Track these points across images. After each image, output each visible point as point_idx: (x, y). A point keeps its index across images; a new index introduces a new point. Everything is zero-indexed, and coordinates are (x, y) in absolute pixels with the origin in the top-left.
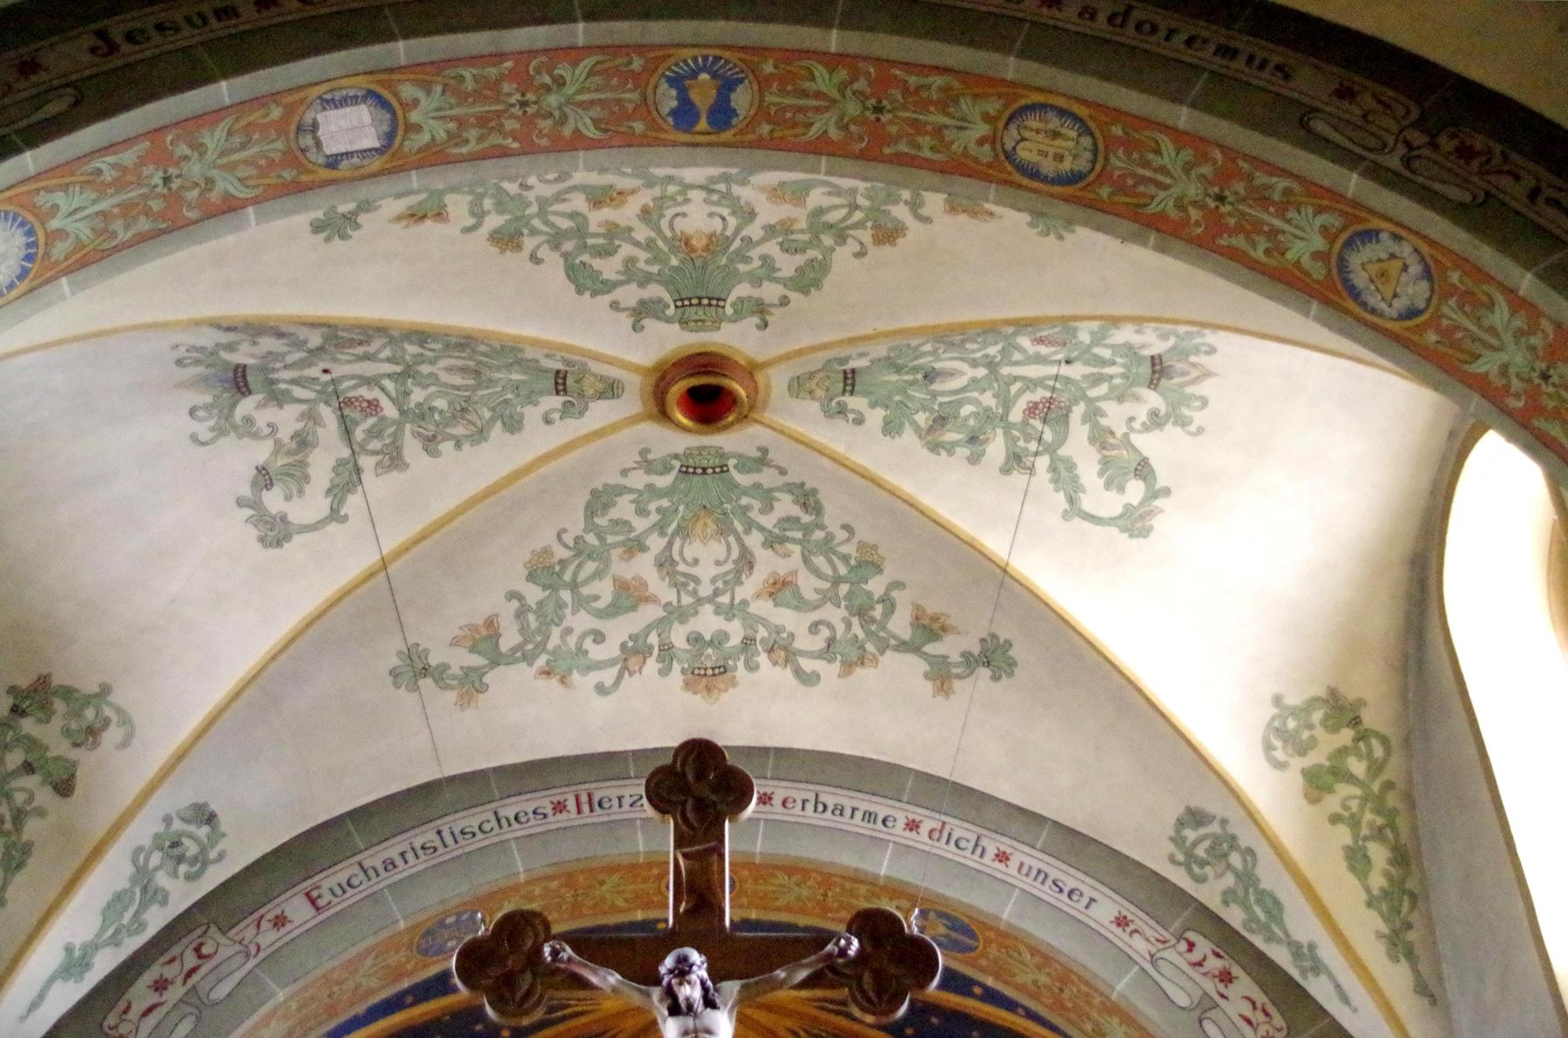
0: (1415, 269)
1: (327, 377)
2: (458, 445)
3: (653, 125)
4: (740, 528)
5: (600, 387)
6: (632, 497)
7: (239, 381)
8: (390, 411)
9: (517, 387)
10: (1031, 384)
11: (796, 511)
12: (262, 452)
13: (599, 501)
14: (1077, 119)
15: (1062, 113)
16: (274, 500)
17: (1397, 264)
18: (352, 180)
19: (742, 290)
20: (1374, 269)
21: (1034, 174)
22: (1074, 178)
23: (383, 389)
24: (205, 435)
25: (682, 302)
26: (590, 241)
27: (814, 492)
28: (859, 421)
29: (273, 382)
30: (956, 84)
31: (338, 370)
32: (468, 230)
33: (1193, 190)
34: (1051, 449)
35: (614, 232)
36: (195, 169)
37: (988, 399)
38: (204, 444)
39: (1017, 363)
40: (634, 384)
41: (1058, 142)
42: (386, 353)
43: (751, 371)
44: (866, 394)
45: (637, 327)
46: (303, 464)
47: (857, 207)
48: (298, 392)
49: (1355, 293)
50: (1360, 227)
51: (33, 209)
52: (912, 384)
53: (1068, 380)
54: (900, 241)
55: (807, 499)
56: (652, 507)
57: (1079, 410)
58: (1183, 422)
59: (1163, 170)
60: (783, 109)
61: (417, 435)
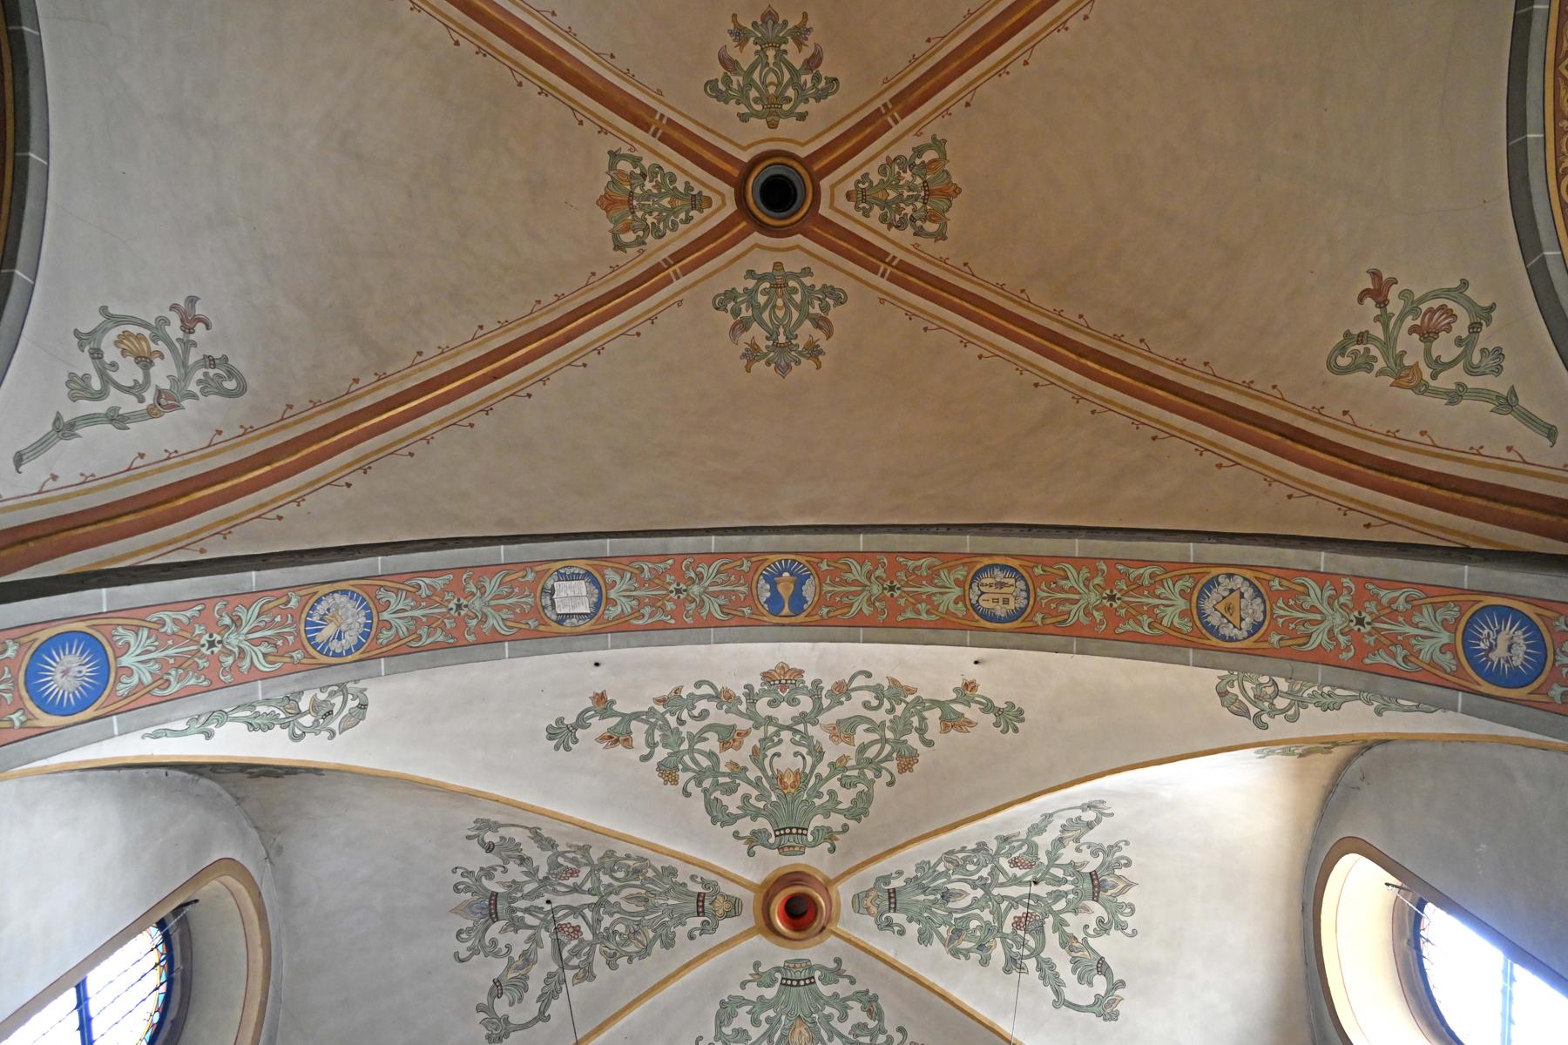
0: (1248, 593)
1: (548, 907)
2: (630, 960)
3: (755, 610)
4: (825, 1037)
5: (726, 905)
6: (748, 1008)
7: (491, 908)
8: (587, 935)
9: (672, 909)
10: (1015, 902)
11: (864, 1018)
12: (498, 967)
13: (726, 1011)
14: (1013, 569)
15: (1003, 568)
16: (502, 1007)
17: (1236, 595)
18: (572, 634)
19: (818, 821)
20: (1221, 607)
21: (990, 617)
22: (1018, 614)
23: (584, 918)
24: (464, 954)
25: (780, 832)
26: (722, 780)
27: (876, 997)
28: (902, 932)
29: (514, 910)
30: (937, 562)
31: (558, 901)
32: (645, 758)
33: (1093, 598)
34: (1035, 953)
35: (737, 771)
36: (477, 604)
37: (987, 915)
38: (462, 961)
39: (1002, 885)
40: (748, 898)
41: (1005, 590)
42: (588, 886)
43: (826, 886)
44: (905, 911)
45: (751, 854)
46: (525, 977)
47: (887, 741)
48: (530, 920)
49: (1213, 630)
50: (1204, 580)
51: (375, 600)
52: (935, 902)
53: (1038, 898)
54: (915, 767)
55: (871, 1005)
56: (763, 1017)
57: (1049, 921)
58: (1122, 927)
59: (1072, 590)
60: (834, 594)
61: (603, 953)
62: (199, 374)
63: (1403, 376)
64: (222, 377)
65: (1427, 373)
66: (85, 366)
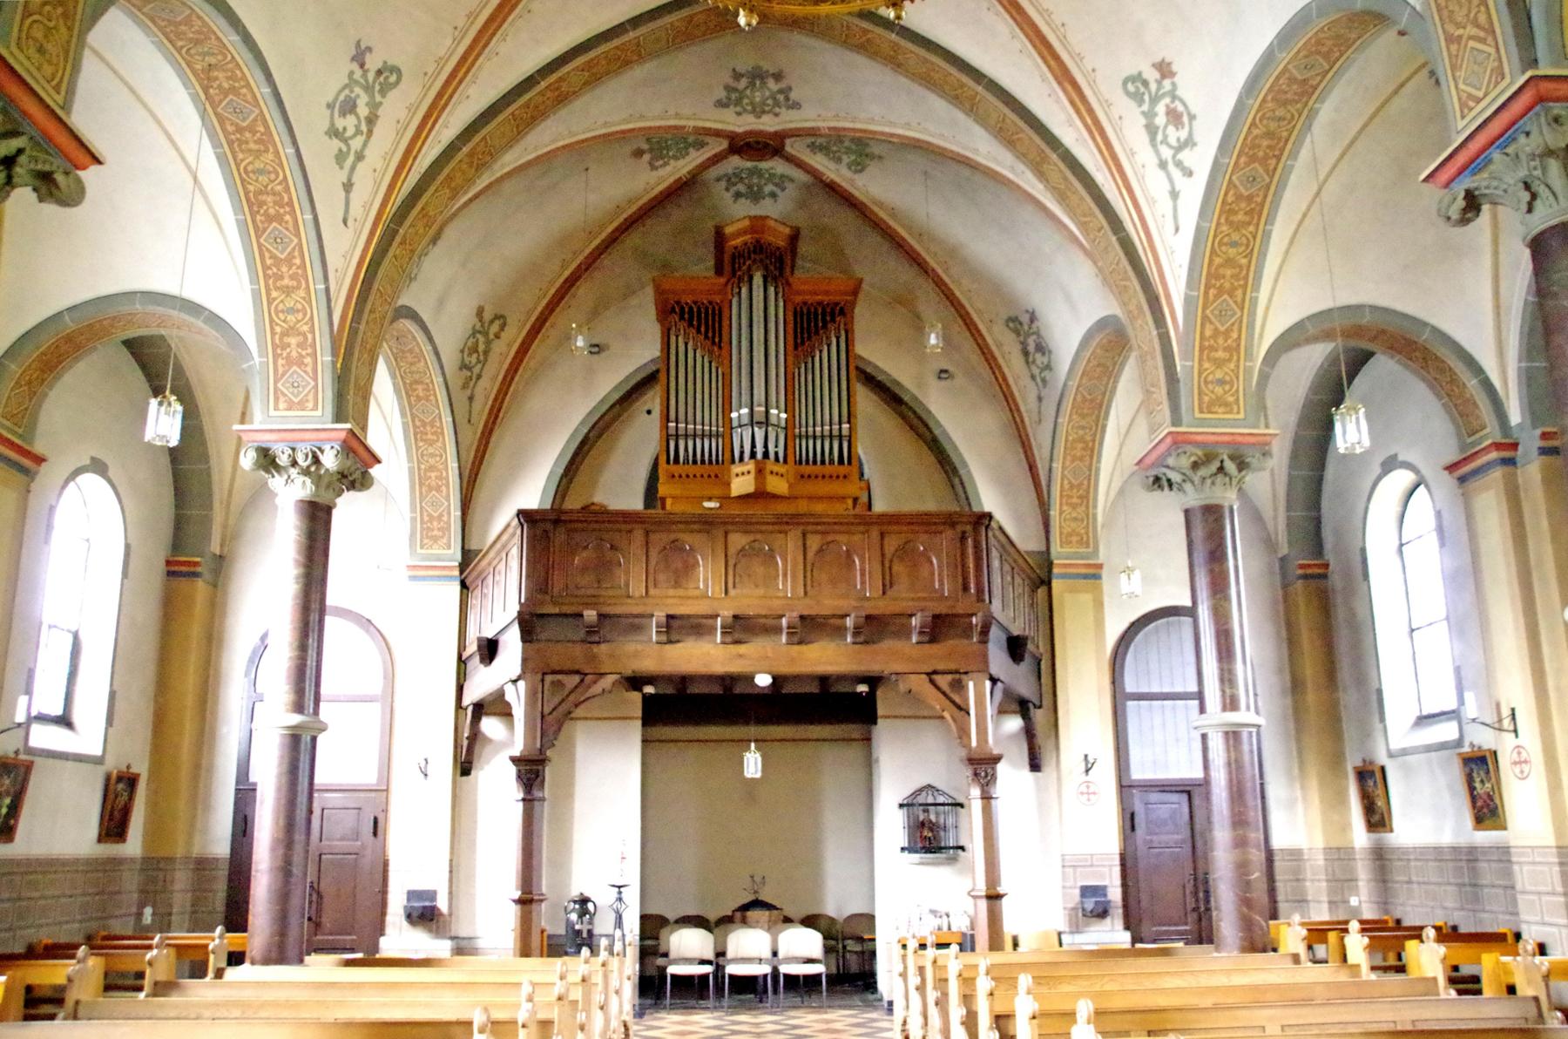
62: (377, 87)
63: (1151, 130)
64: (388, 76)
65: (1160, 137)
66: (336, 144)
